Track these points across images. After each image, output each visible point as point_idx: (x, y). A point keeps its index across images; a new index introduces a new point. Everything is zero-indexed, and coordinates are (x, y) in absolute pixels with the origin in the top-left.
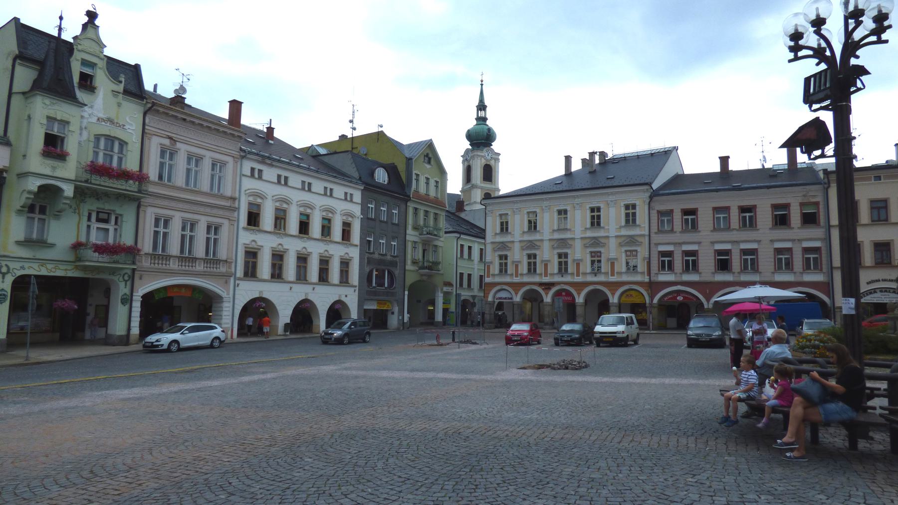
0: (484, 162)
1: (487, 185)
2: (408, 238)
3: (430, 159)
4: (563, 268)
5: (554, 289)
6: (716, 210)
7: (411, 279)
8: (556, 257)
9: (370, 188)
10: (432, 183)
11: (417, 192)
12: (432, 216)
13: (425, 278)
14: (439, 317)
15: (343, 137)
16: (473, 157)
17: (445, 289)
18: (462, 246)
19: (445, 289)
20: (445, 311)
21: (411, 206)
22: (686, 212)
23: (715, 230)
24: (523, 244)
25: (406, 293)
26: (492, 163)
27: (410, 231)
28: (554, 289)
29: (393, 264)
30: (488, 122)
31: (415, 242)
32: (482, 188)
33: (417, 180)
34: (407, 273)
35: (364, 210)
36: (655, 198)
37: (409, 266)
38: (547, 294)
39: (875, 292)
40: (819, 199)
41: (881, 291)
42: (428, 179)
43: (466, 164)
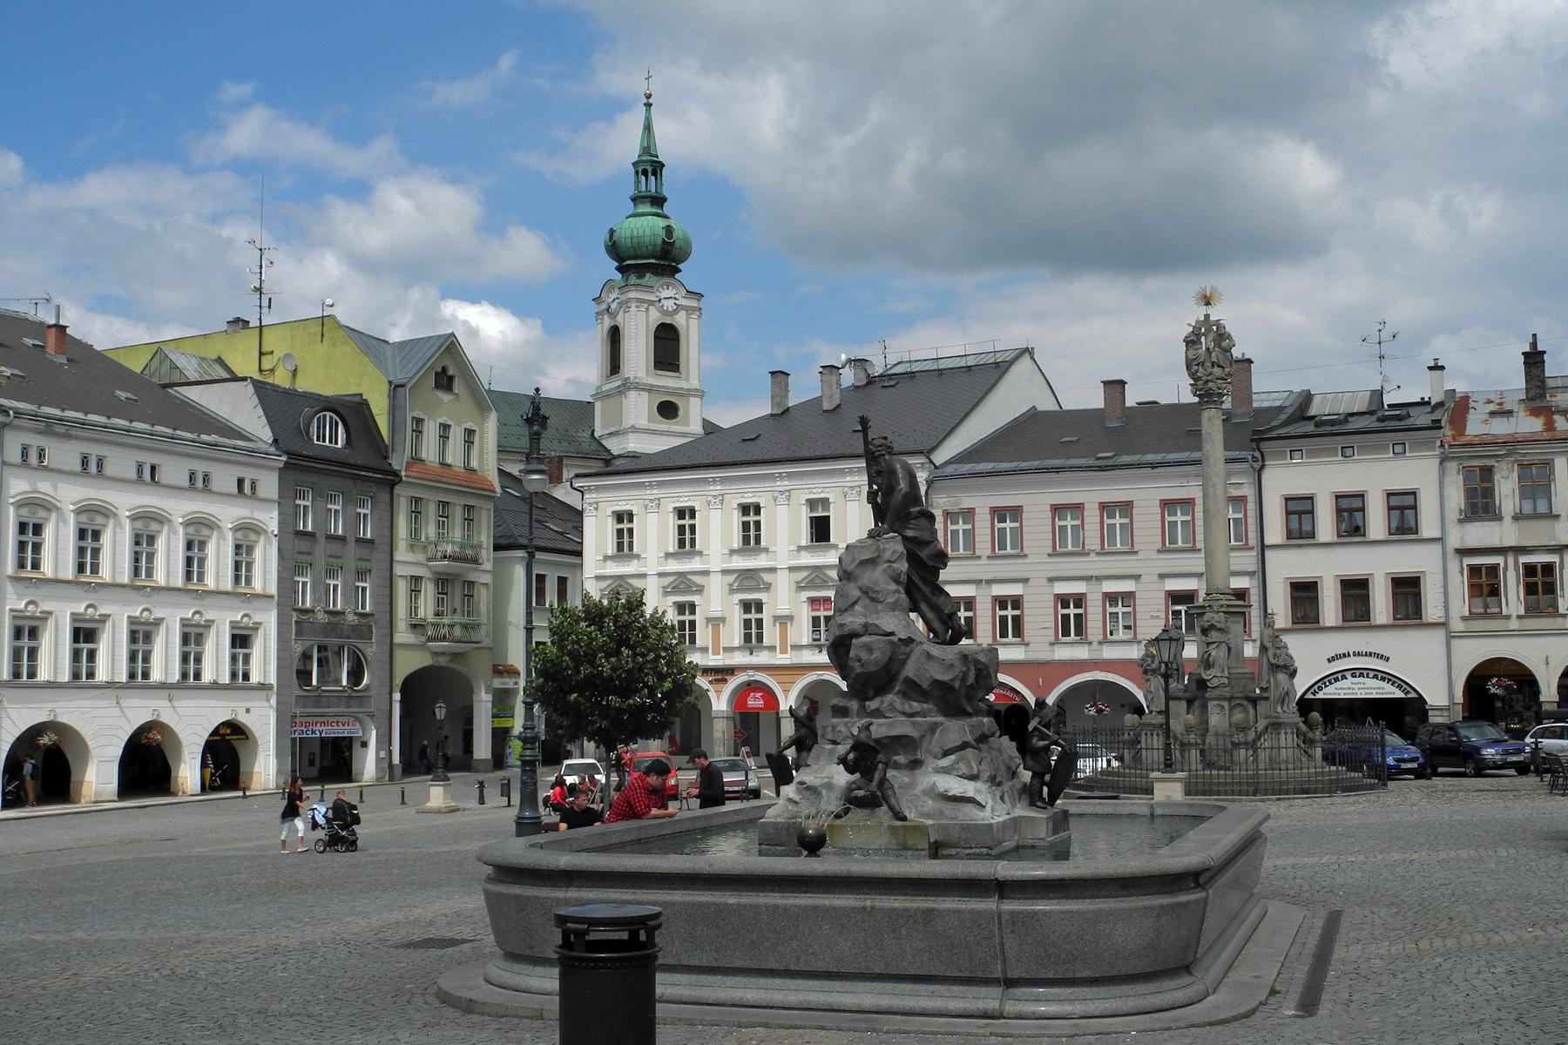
0: (655, 317)
1: (667, 380)
2: (399, 570)
3: (451, 378)
4: (753, 636)
5: (734, 682)
6: (1057, 510)
7: (407, 664)
8: (737, 610)
9: (302, 467)
10: (456, 435)
11: (416, 460)
12: (458, 514)
13: (443, 661)
14: (482, 749)
15: (240, 323)
16: (625, 305)
17: (498, 683)
18: (541, 579)
19: (498, 683)
20: (500, 737)
21: (403, 495)
22: (999, 513)
23: (1054, 554)
24: (667, 581)
25: (397, 696)
26: (680, 320)
27: (402, 553)
28: (734, 682)
29: (363, 629)
30: (667, 208)
31: (416, 579)
32: (650, 389)
33: (418, 432)
34: (398, 653)
35: (289, 517)
36: (937, 484)
37: (403, 635)
38: (718, 692)
39: (1344, 677)
40: (1248, 491)
41: (1354, 676)
42: (445, 427)
43: (607, 322)
